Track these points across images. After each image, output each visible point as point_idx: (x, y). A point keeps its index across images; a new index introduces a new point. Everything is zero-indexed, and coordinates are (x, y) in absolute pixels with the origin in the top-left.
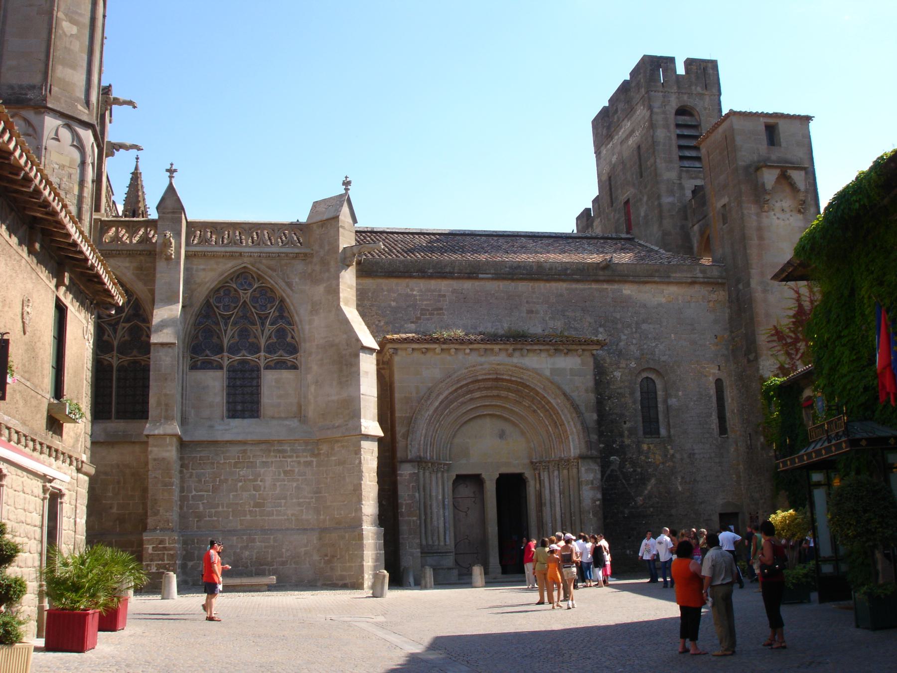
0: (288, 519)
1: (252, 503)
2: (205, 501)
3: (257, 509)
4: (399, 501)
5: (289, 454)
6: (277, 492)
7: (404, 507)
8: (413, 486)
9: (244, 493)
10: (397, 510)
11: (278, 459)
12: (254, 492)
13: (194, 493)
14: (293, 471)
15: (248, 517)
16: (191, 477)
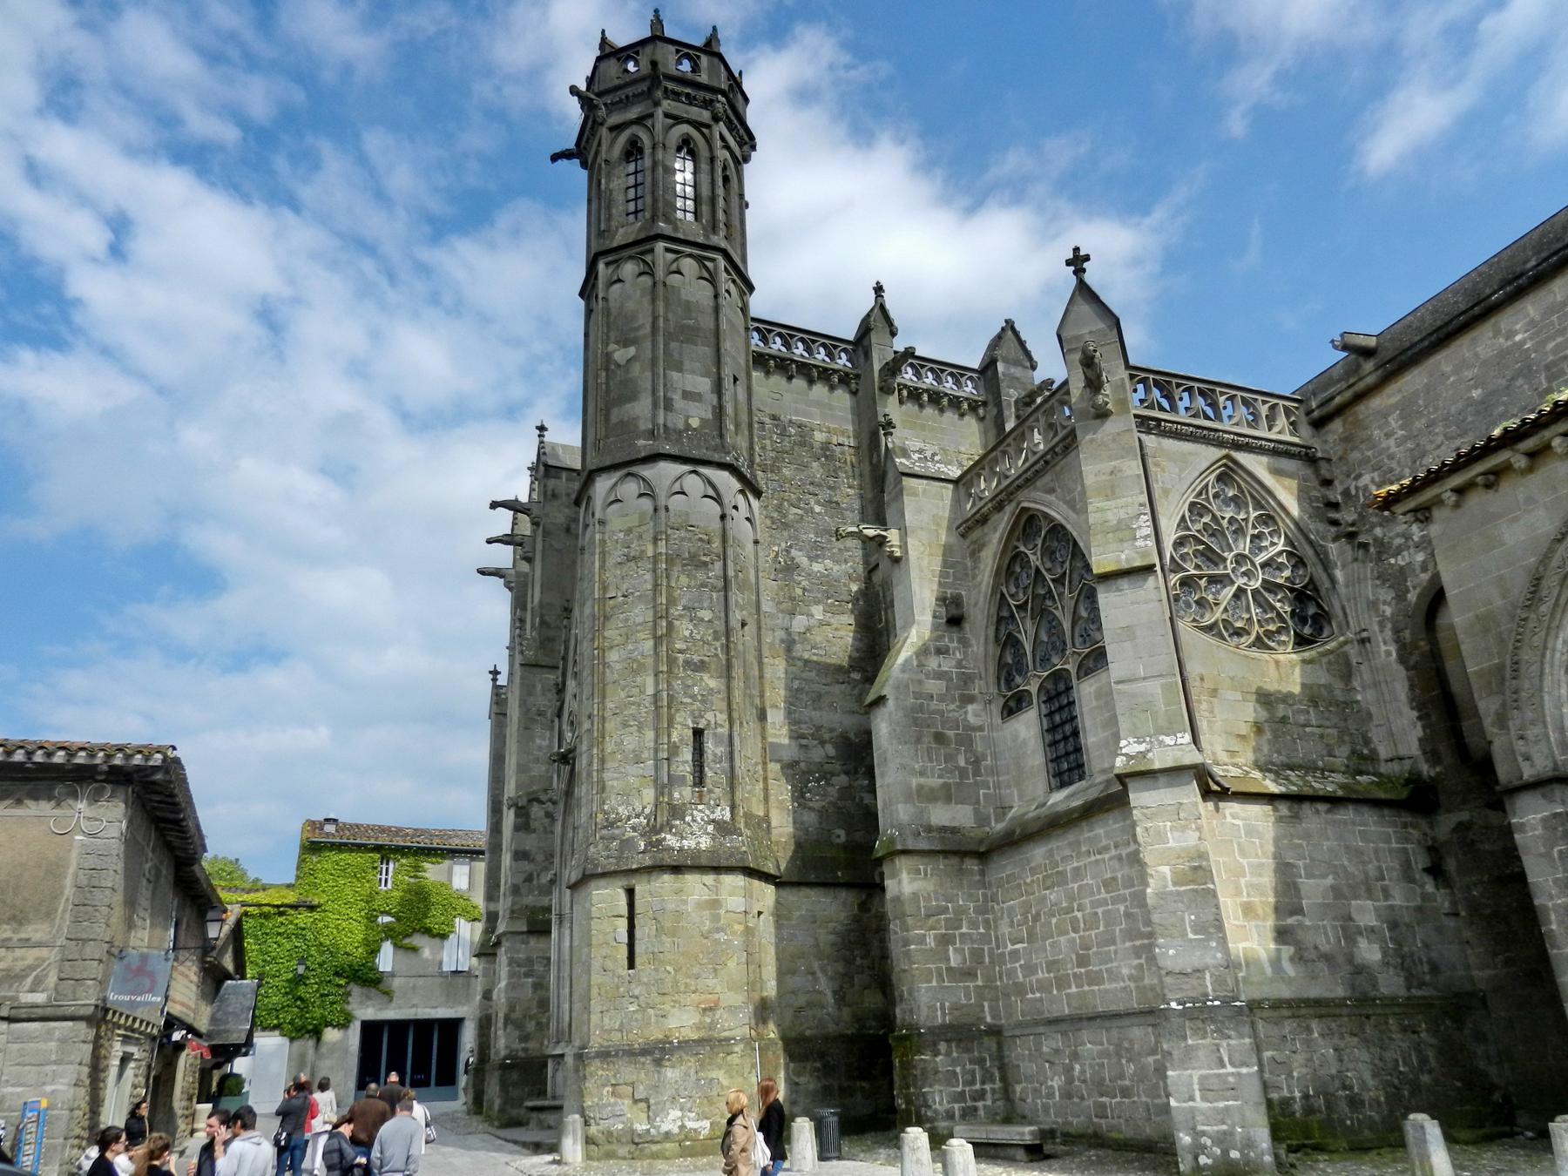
0: (1125, 988)
1: (1074, 957)
2: (1022, 962)
3: (1083, 970)
4: (1536, 902)
5: (1104, 842)
6: (1101, 929)
7: (1553, 917)
8: (1560, 852)
9: (1062, 939)
10: (1539, 927)
11: (1093, 858)
12: (1074, 935)
13: (1010, 947)
14: (1114, 879)
15: (1074, 989)
16: (1002, 918)
